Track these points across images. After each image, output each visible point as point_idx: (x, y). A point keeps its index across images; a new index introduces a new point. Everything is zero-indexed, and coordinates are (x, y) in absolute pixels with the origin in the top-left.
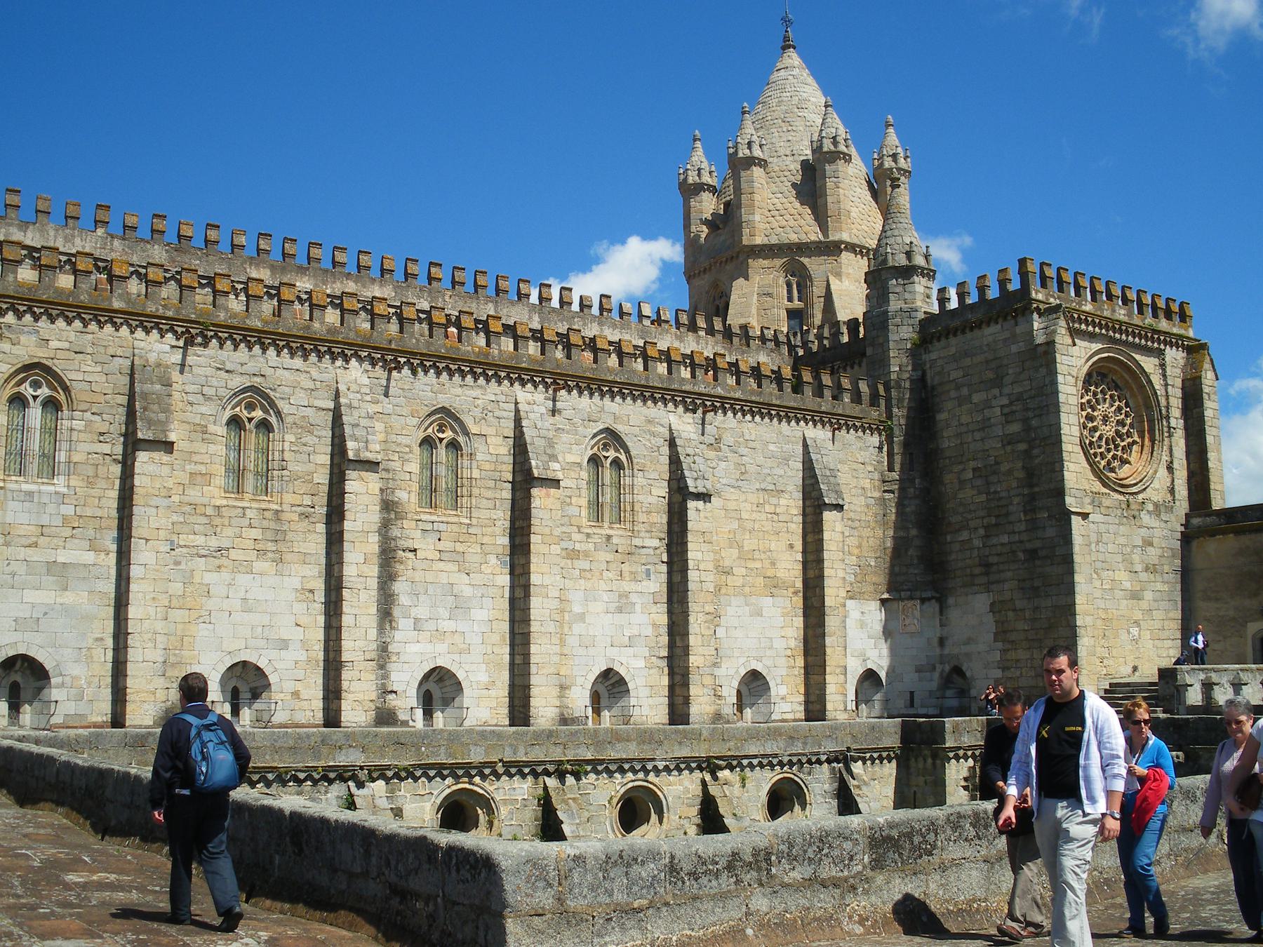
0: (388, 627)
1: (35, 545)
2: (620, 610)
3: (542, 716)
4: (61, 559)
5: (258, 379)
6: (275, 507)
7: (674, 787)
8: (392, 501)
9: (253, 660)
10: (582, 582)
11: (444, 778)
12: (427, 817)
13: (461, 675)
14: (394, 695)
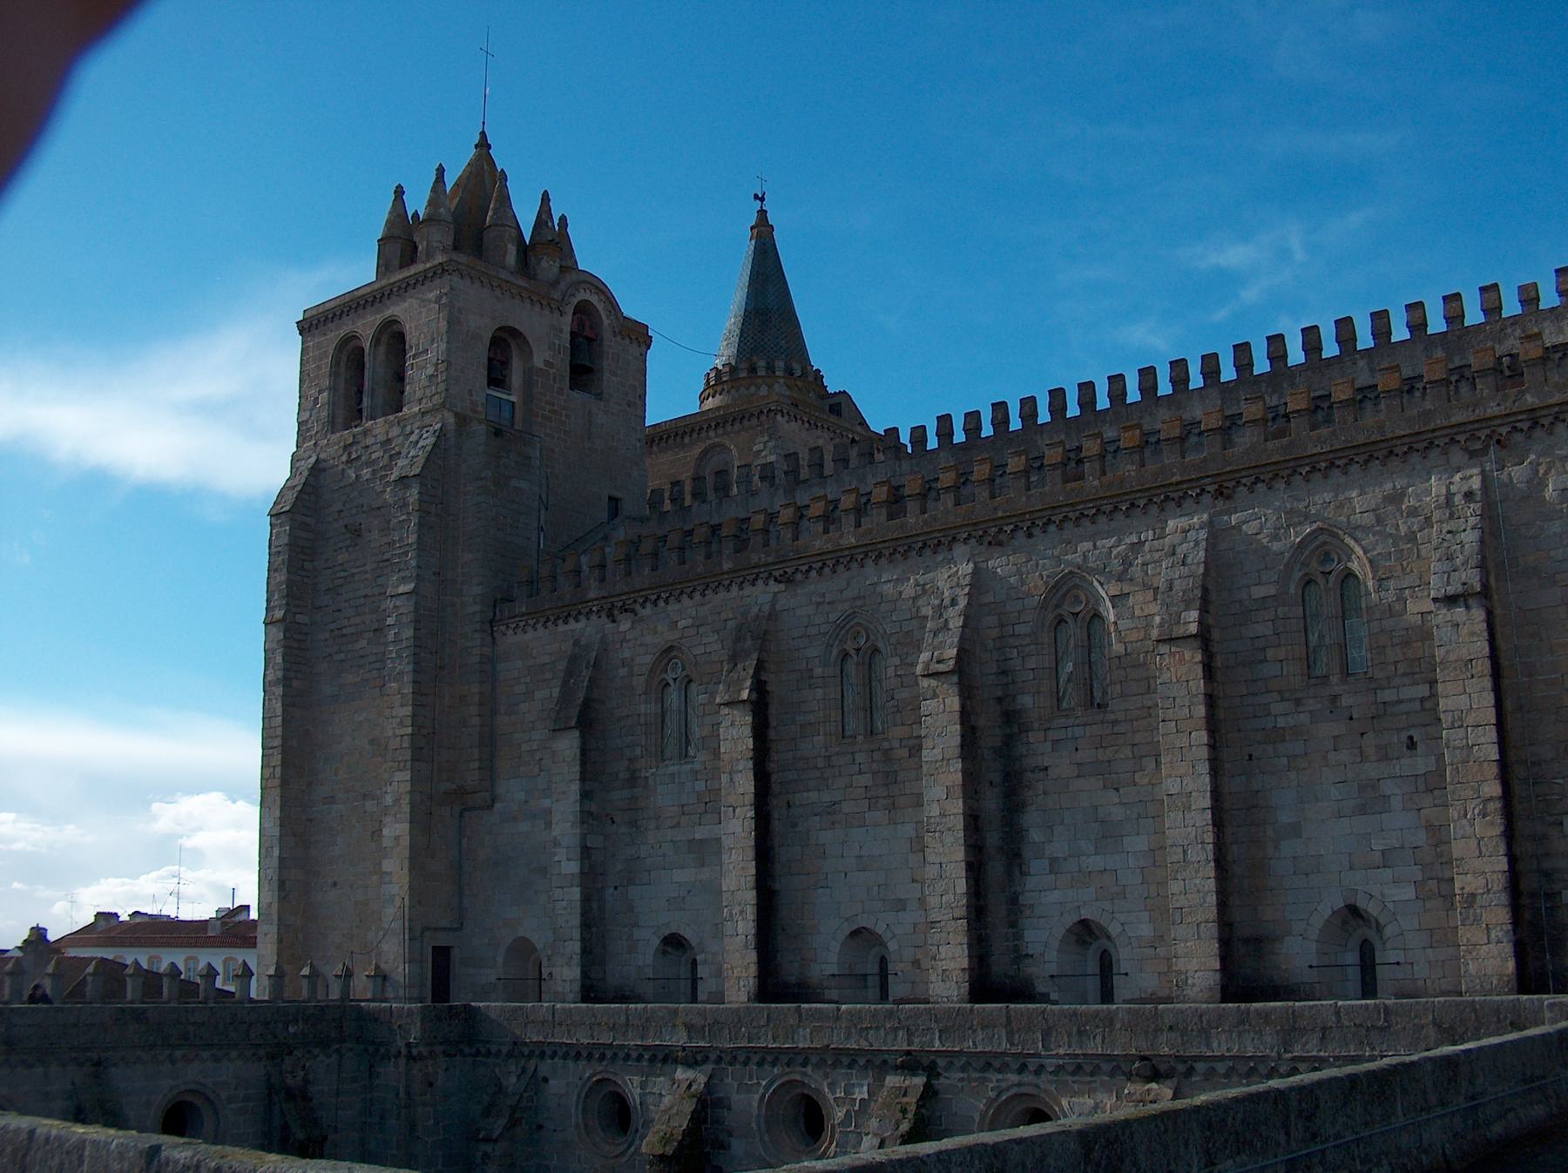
0: (1017, 873)
1: (678, 825)
2: (1363, 810)
3: (1194, 985)
4: (698, 836)
5: (859, 603)
6: (886, 745)
7: (1082, 1100)
8: (1013, 711)
9: (870, 925)
10: (1293, 775)
11: (773, 1064)
12: (755, 1112)
13: (1114, 930)
14: (1030, 960)
